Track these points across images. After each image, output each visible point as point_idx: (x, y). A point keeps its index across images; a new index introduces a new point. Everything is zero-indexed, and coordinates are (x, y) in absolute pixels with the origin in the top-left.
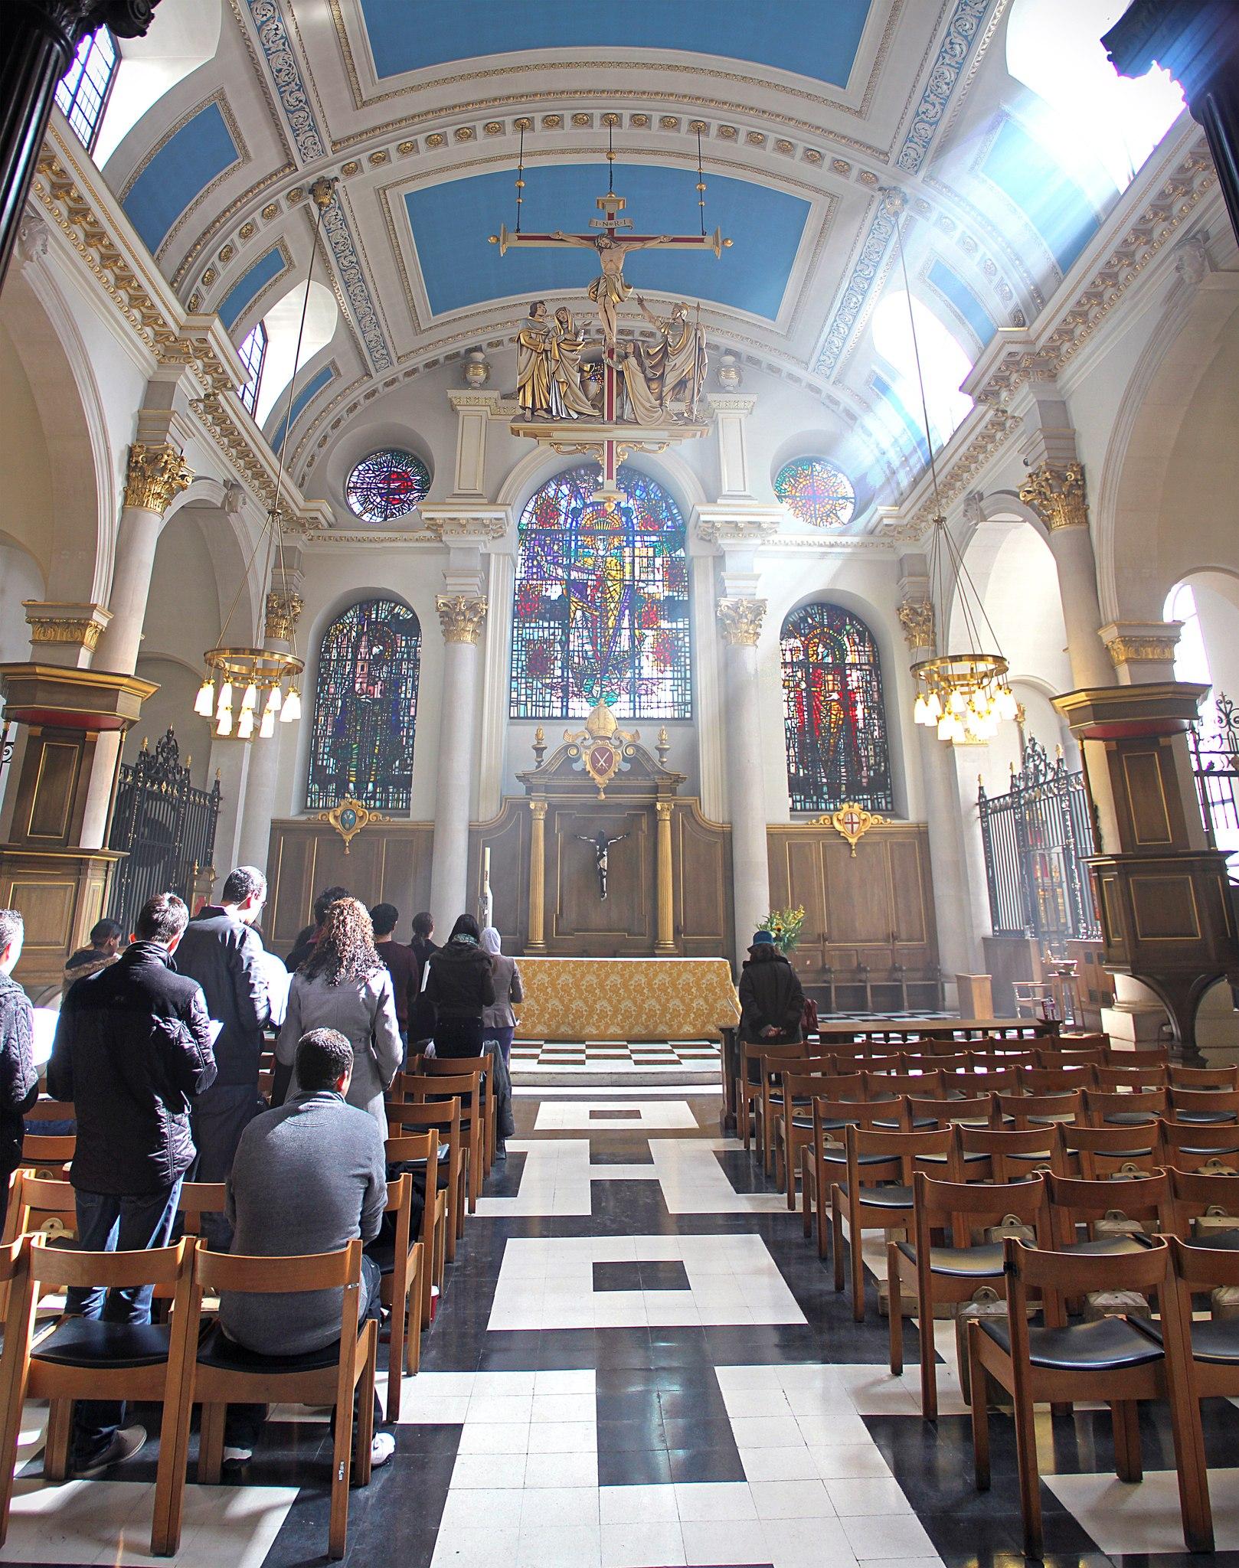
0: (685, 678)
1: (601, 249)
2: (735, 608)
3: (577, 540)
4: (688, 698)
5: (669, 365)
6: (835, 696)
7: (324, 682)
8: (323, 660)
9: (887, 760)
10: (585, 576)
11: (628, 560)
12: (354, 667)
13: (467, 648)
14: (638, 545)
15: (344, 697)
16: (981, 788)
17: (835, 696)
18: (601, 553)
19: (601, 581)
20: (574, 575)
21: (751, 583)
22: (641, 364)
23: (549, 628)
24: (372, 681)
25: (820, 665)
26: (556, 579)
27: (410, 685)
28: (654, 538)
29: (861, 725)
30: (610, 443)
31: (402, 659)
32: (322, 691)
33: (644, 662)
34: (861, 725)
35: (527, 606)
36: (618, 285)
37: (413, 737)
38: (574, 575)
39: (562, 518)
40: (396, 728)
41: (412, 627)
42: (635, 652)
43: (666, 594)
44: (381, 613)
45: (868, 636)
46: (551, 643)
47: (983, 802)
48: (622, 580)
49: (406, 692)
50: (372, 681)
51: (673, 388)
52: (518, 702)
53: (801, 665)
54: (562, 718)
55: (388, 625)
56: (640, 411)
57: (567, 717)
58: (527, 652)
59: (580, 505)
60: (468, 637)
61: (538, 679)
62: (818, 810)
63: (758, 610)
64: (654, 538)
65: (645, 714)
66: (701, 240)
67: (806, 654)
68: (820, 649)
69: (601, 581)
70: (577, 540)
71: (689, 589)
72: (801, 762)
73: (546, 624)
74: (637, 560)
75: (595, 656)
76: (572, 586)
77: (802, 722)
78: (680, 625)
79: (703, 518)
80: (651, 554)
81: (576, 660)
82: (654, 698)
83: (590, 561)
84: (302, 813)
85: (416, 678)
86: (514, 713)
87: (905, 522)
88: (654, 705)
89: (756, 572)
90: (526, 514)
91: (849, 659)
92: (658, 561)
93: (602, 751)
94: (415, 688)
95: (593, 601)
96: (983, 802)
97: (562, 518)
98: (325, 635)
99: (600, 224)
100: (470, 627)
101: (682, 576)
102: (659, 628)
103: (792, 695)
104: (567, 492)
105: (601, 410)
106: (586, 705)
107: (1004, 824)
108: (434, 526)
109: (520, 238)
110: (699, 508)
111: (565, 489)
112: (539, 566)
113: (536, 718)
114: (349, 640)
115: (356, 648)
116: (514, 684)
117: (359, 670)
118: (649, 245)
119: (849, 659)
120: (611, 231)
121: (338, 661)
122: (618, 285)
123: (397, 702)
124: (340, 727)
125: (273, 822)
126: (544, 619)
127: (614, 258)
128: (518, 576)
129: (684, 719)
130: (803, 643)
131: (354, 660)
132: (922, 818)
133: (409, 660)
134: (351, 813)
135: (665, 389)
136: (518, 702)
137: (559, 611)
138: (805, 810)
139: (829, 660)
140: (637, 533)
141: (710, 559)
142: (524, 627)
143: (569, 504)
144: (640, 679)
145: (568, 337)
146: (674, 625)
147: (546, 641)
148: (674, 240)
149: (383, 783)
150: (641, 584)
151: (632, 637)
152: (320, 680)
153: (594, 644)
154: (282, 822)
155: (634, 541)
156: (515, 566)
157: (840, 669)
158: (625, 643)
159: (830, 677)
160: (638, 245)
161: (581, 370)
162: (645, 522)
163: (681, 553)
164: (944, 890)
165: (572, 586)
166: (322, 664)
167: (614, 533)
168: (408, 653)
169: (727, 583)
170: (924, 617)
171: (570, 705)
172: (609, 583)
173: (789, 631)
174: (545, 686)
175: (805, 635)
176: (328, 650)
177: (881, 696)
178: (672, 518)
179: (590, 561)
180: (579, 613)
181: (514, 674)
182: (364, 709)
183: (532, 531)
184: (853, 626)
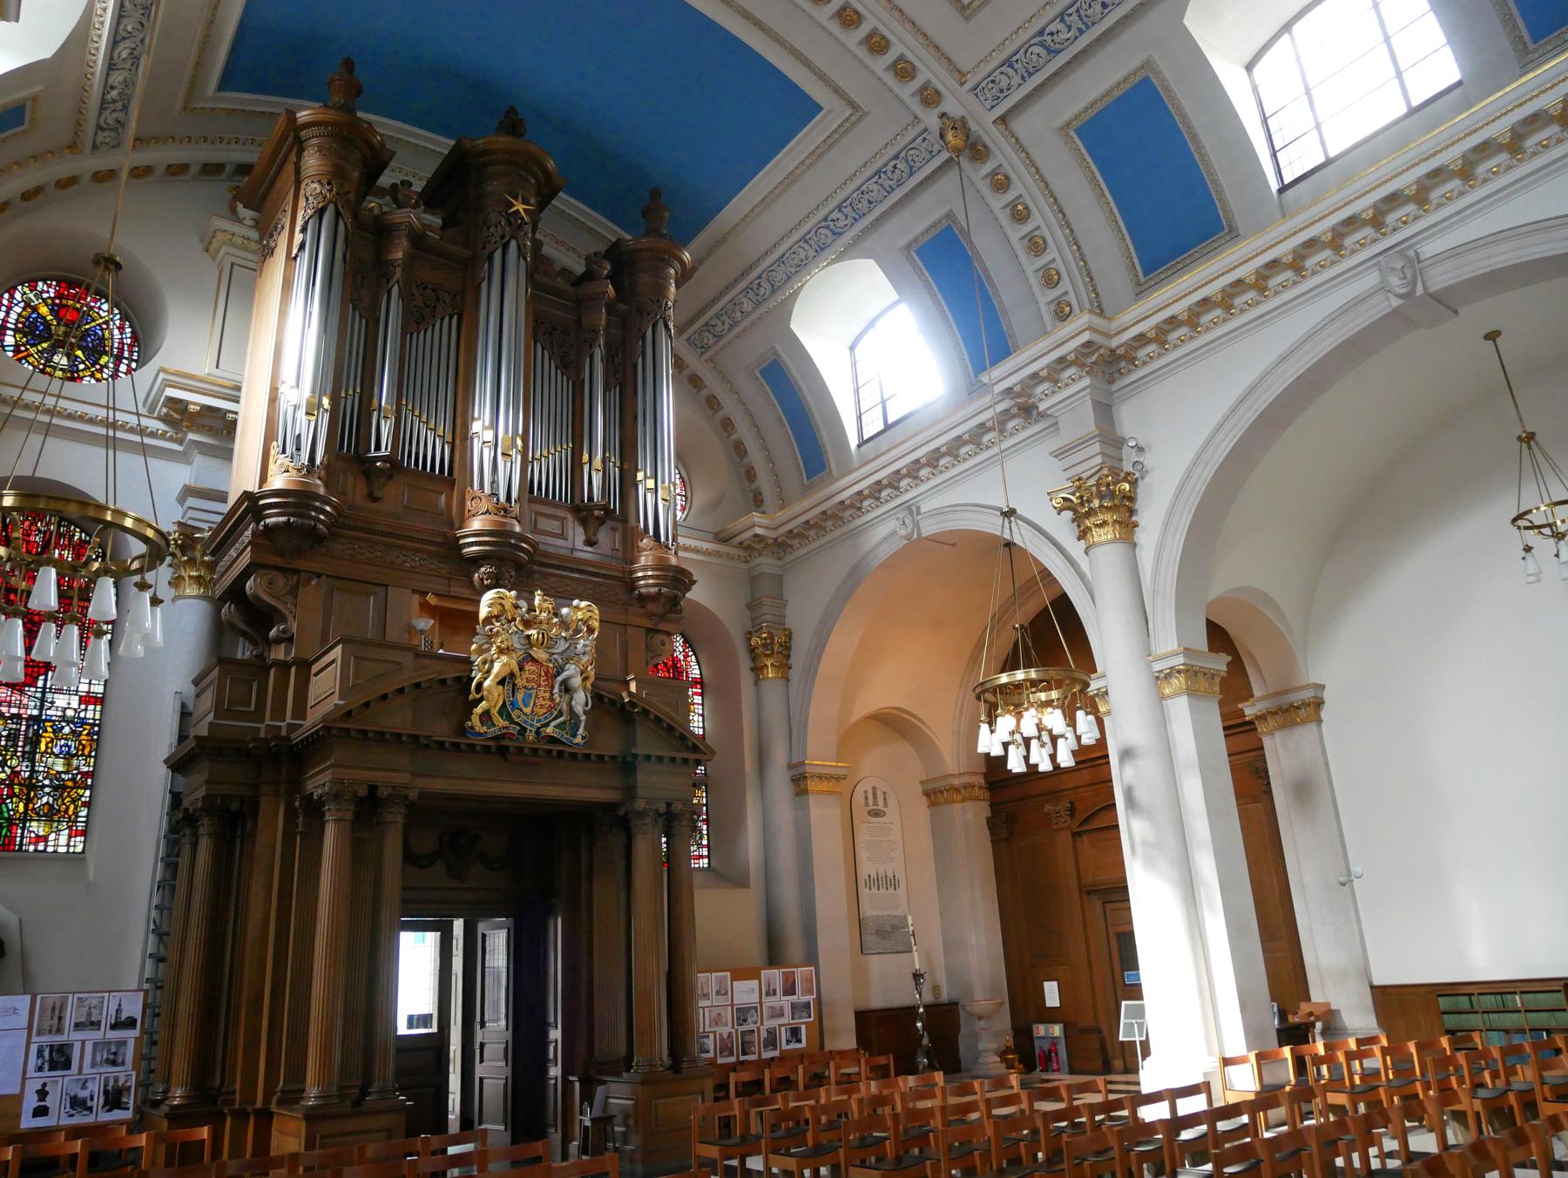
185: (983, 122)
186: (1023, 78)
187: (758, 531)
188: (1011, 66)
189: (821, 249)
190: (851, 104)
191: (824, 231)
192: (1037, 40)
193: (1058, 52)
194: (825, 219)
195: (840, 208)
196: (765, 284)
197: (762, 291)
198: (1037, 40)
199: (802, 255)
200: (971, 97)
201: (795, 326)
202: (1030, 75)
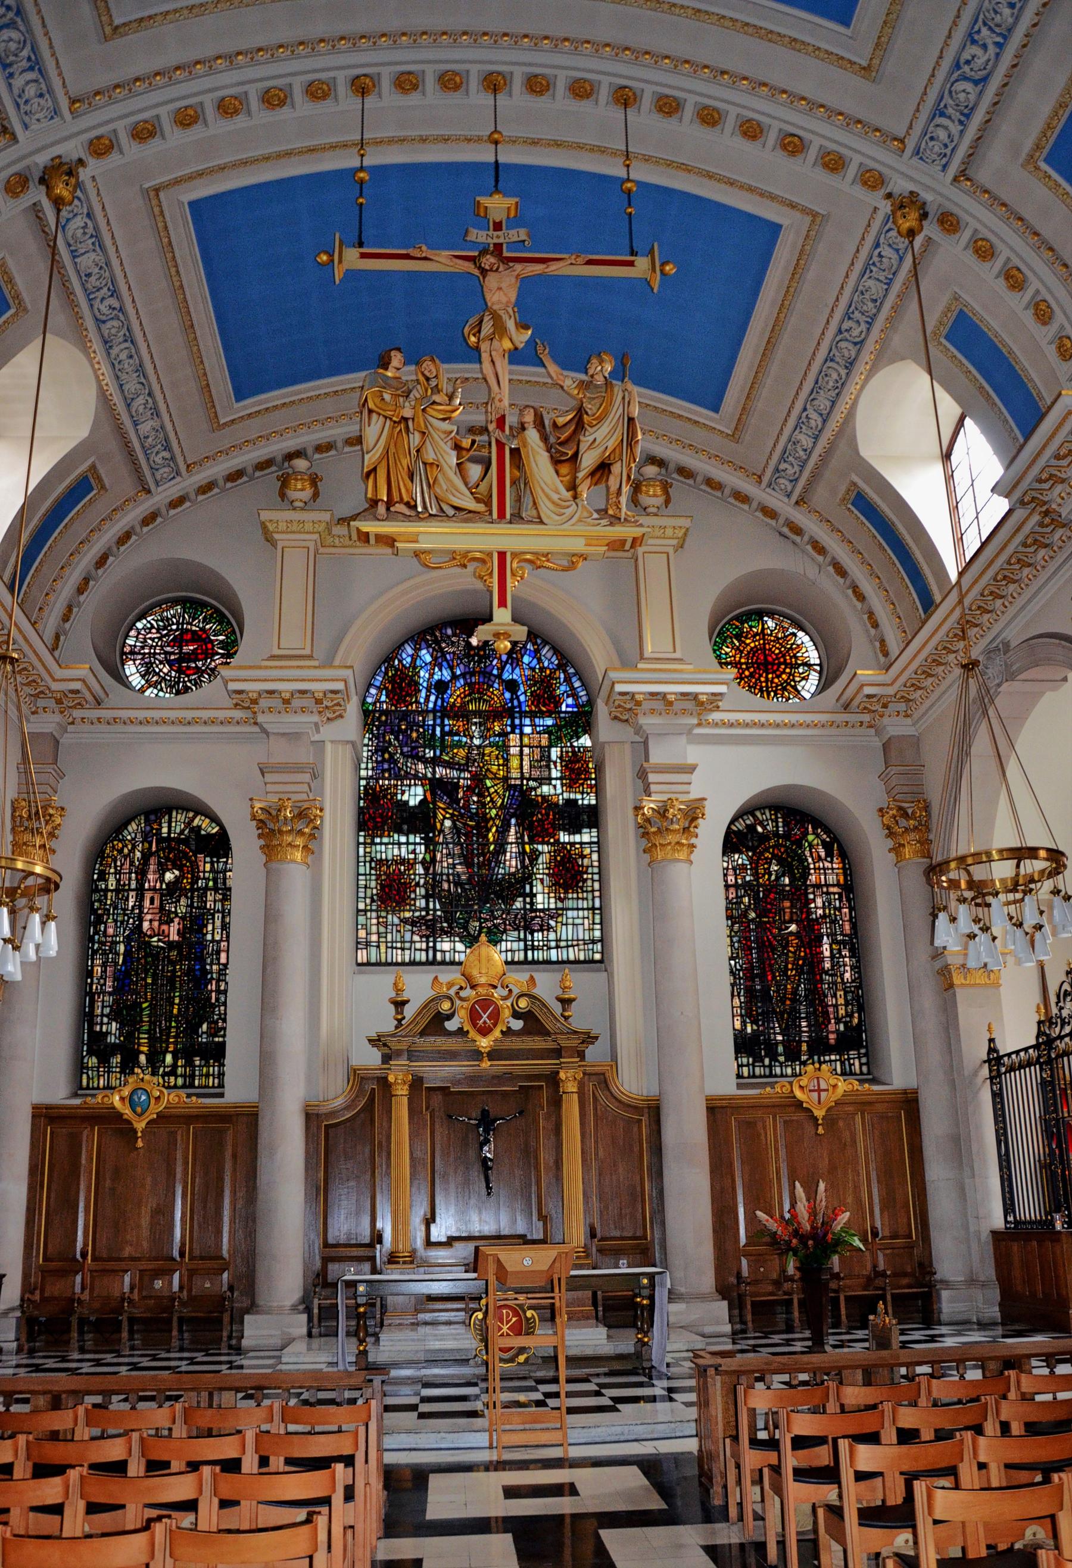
0: (593, 909)
1: (484, 272)
2: (662, 812)
3: (442, 726)
4: (597, 934)
5: (586, 440)
7: (99, 920)
8: (97, 890)
9: (861, 1009)
10: (455, 774)
11: (514, 751)
12: (140, 898)
13: (295, 868)
14: (527, 730)
15: (128, 940)
16: (991, 1040)
17: (793, 927)
18: (477, 742)
19: (478, 780)
20: (440, 771)
21: (683, 778)
22: (545, 438)
23: (408, 843)
24: (166, 918)
25: (774, 887)
26: (416, 777)
27: (218, 923)
28: (549, 722)
29: (827, 965)
30: (502, 555)
31: (206, 888)
32: (96, 932)
33: (538, 888)
34: (827, 965)
35: (377, 814)
36: (511, 325)
37: (225, 992)
38: (440, 771)
39: (423, 694)
40: (200, 979)
41: (219, 845)
42: (526, 877)
43: (566, 796)
44: (175, 825)
45: (837, 846)
46: (410, 864)
47: (994, 1059)
48: (506, 779)
49: (213, 931)
50: (166, 918)
51: (592, 474)
52: (368, 944)
53: (746, 885)
54: (428, 963)
55: (186, 842)
56: (546, 509)
57: (433, 962)
58: (378, 877)
59: (446, 675)
60: (298, 855)
61: (394, 912)
62: (771, 1075)
63: (693, 813)
64: (549, 722)
65: (539, 955)
66: (631, 264)
67: (756, 874)
68: (774, 868)
69: (478, 780)
70: (442, 726)
71: (598, 790)
72: (748, 1014)
73: (403, 839)
74: (526, 750)
75: (470, 880)
76: (436, 786)
77: (750, 962)
78: (586, 838)
79: (619, 688)
80: (544, 742)
81: (445, 886)
82: (552, 936)
83: (462, 753)
84: (75, 1095)
85: (225, 913)
86: (362, 956)
87: (891, 691)
88: (553, 944)
89: (690, 761)
90: (373, 691)
92: (555, 753)
93: (486, 1003)
94: (225, 926)
95: (467, 807)
96: (994, 1059)
97: (423, 694)
98: (100, 853)
99: (480, 236)
100: (300, 841)
101: (587, 771)
102: (557, 841)
104: (428, 659)
105: (488, 503)
106: (460, 946)
107: (1023, 1089)
108: (246, 702)
109: (364, 256)
110: (613, 675)
111: (426, 656)
112: (392, 760)
113: (391, 964)
114: (132, 863)
115: (142, 873)
116: (362, 919)
117: (147, 903)
118: (553, 268)
120: (498, 247)
121: (117, 891)
122: (511, 325)
123: (202, 944)
124: (123, 980)
125: (35, 1107)
126: (400, 832)
127: (503, 285)
128: (363, 773)
129: (593, 961)
130: (750, 859)
131: (140, 891)
132: (912, 1083)
133: (216, 889)
134: (142, 1095)
135: (580, 475)
136: (368, 944)
137: (418, 821)
138: (754, 1076)
140: (523, 714)
141: (627, 746)
142: (373, 843)
143: (432, 675)
144: (532, 910)
145: (437, 398)
146: (577, 838)
147: (403, 861)
148: (590, 262)
149: (187, 1053)
150: (531, 783)
151: (522, 853)
152: (92, 915)
153: (468, 864)
154: (49, 1107)
155: (521, 726)
156: (359, 761)
157: (800, 895)
158: (511, 862)
159: (787, 904)
160: (538, 268)
161: (457, 447)
162: (536, 698)
163: (585, 741)
164: (938, 1172)
165: (436, 786)
166: (95, 897)
167: (497, 714)
168: (215, 880)
169: (652, 777)
170: (913, 819)
171: (438, 946)
172: (489, 783)
173: (732, 842)
174: (405, 921)
175: (753, 849)
176: (103, 876)
177: (854, 926)
178: (574, 695)
179: (462, 753)
180: (448, 823)
181: (361, 906)
182: (155, 955)
183: (383, 712)
184: (818, 836)
185: (937, 188)
186: (961, 122)
187: (868, 690)
188: (942, 114)
189: (850, 365)
190: (805, 211)
191: (843, 344)
192: (955, 75)
193: (985, 79)
194: (840, 332)
195: (848, 316)
196: (814, 416)
197: (813, 423)
198: (955, 75)
199: (835, 376)
200: (915, 161)
201: (868, 451)
202: (967, 116)
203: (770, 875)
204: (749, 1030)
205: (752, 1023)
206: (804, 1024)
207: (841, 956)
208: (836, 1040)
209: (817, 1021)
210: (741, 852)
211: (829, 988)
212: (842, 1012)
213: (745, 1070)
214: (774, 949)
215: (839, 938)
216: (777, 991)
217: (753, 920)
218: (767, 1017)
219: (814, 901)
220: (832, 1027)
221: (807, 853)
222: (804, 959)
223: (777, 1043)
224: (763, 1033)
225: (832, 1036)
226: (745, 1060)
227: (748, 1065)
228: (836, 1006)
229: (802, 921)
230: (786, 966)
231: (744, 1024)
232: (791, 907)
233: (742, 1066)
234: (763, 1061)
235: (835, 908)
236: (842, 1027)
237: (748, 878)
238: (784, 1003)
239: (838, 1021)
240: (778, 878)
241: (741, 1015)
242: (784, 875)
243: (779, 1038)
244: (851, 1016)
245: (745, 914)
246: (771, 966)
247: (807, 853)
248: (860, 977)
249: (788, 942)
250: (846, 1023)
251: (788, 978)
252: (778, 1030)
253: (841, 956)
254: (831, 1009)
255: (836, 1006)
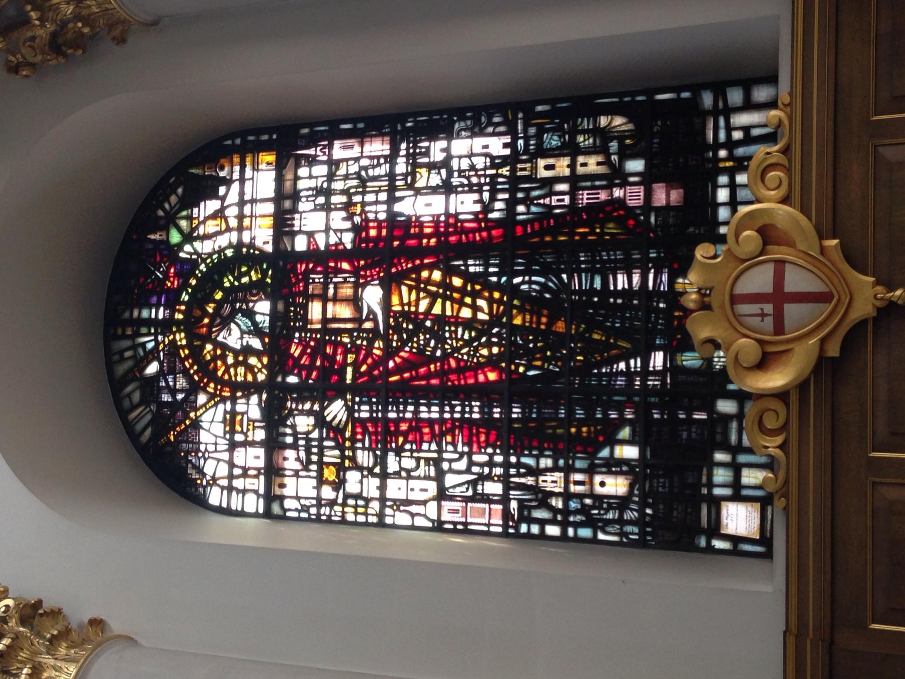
6: (372, 295)
17: (372, 295)
67: (248, 389)
68: (233, 337)
91: (262, 236)
103: (364, 458)
119: (262, 236)
139: (263, 307)
157: (287, 273)
159: (315, 310)
175: (194, 389)
203: (248, 351)
204: (630, 452)
205: (613, 442)
206: (621, 281)
207: (446, 164)
208: (671, 183)
209: (614, 244)
210: (196, 425)
211: (528, 201)
212: (591, 164)
213: (751, 477)
214: (421, 358)
215: (401, 167)
216: (530, 356)
217: (350, 411)
218: (601, 395)
219: (310, 235)
220: (634, 196)
221: (205, 247)
222: (449, 271)
223: (672, 368)
224: (643, 411)
225: (660, 197)
226: (721, 475)
227: (736, 468)
228: (575, 181)
229: (355, 272)
230: (468, 324)
231: (614, 466)
232: (324, 299)
233: (736, 484)
234: (726, 418)
235: (331, 177)
236: (636, 165)
237: (255, 412)
238: (562, 340)
239: (616, 176)
240: (257, 331)
241: (591, 471)
242: (250, 314)
243: (658, 360)
244: (605, 135)
245: (336, 431)
246: (463, 369)
247: (205, 247)
248: (501, 108)
249: (406, 315)
250: (626, 154)
251: (495, 320)
252: (636, 363)
253: (446, 164)
254: (584, 198)
255: (575, 181)
